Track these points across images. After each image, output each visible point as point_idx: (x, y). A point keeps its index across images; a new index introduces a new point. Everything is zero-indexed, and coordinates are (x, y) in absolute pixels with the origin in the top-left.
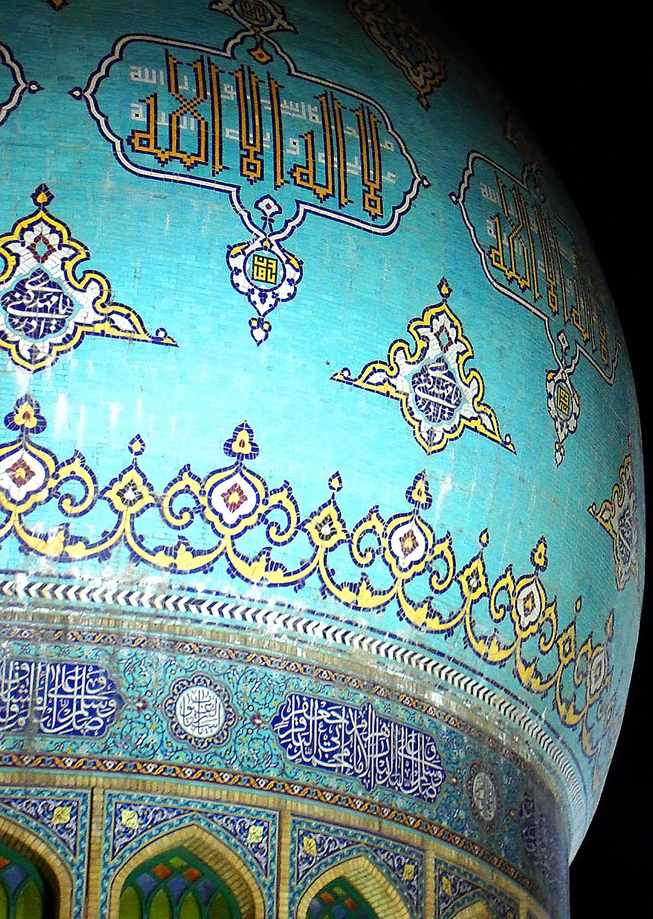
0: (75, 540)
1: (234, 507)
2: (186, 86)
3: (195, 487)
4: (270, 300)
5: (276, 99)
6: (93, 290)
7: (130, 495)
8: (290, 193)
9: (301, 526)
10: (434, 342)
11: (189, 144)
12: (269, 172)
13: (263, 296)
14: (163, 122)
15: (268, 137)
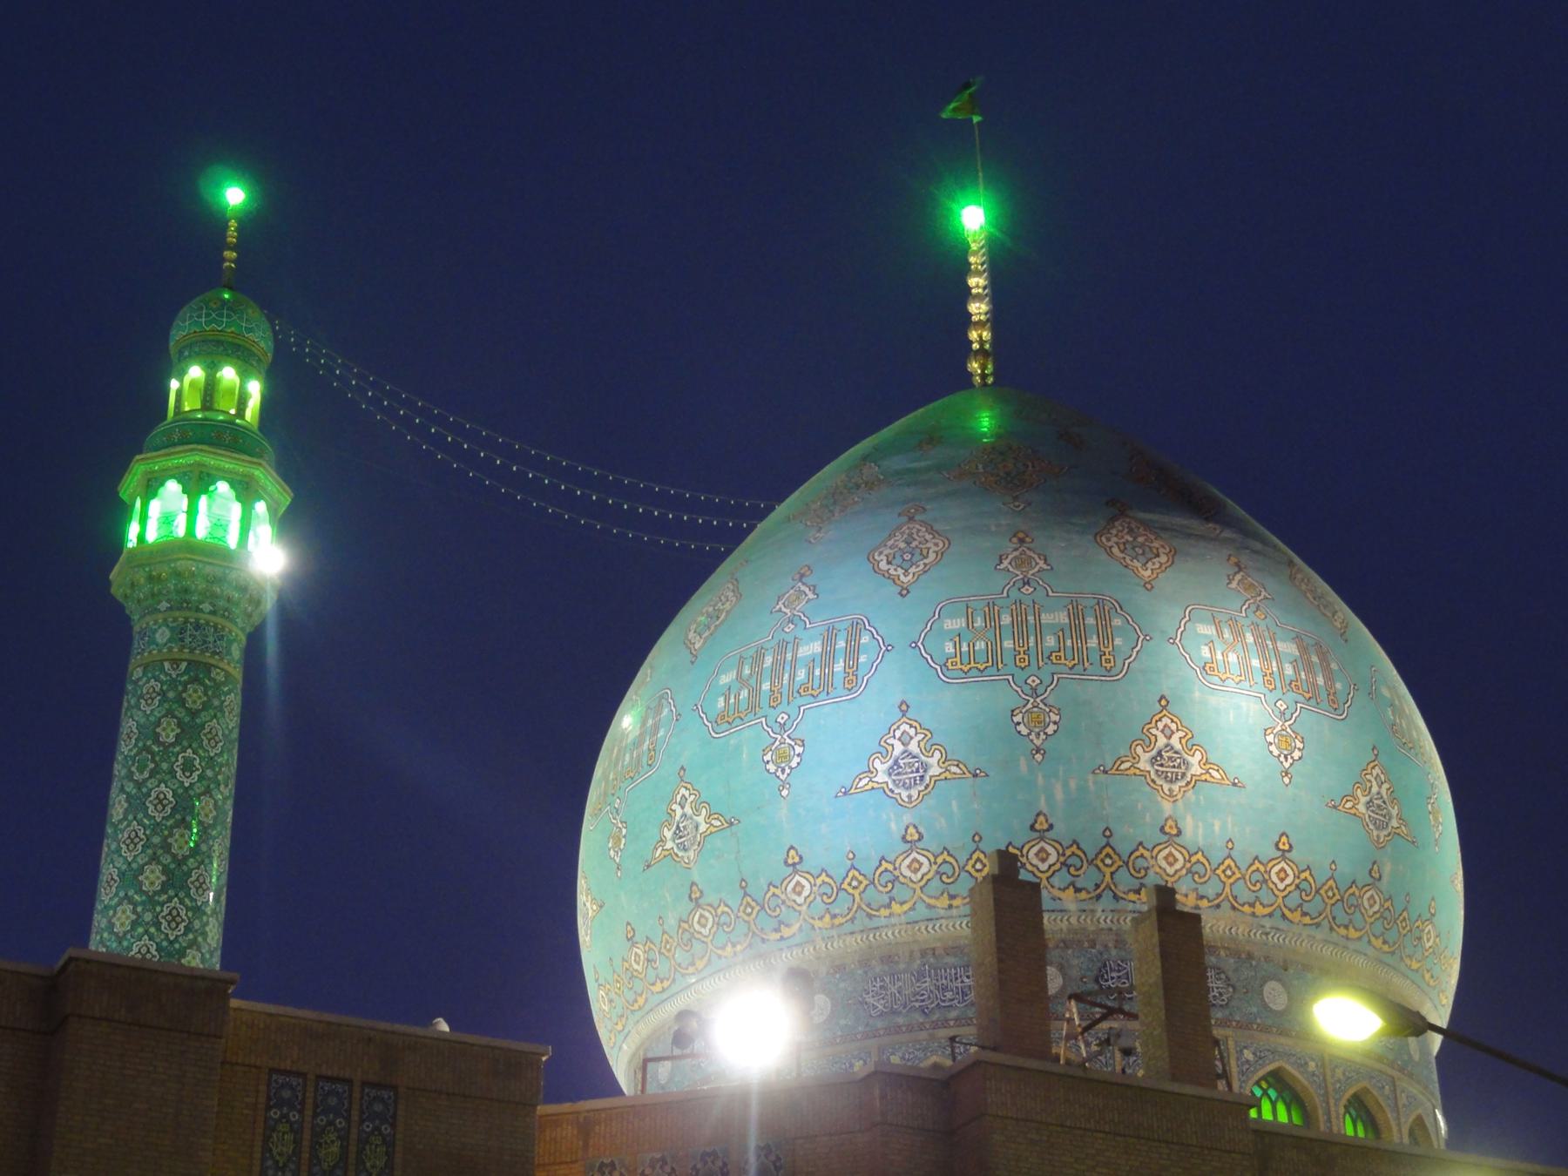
2: (1227, 635)
4: (1043, 736)
6: (937, 755)
7: (1229, 873)
15: (1032, 639)
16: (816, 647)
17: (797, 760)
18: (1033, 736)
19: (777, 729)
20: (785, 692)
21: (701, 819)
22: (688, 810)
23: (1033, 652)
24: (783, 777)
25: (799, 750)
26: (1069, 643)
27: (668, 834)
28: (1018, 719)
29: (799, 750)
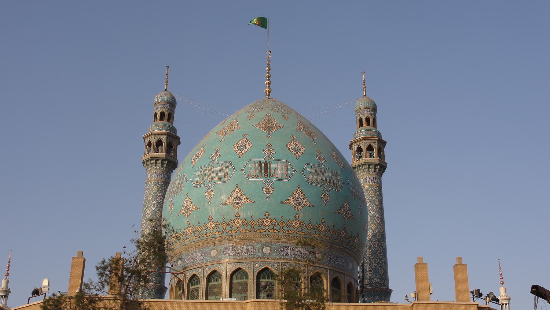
5: (270, 165)
11: (257, 174)
16: (218, 169)
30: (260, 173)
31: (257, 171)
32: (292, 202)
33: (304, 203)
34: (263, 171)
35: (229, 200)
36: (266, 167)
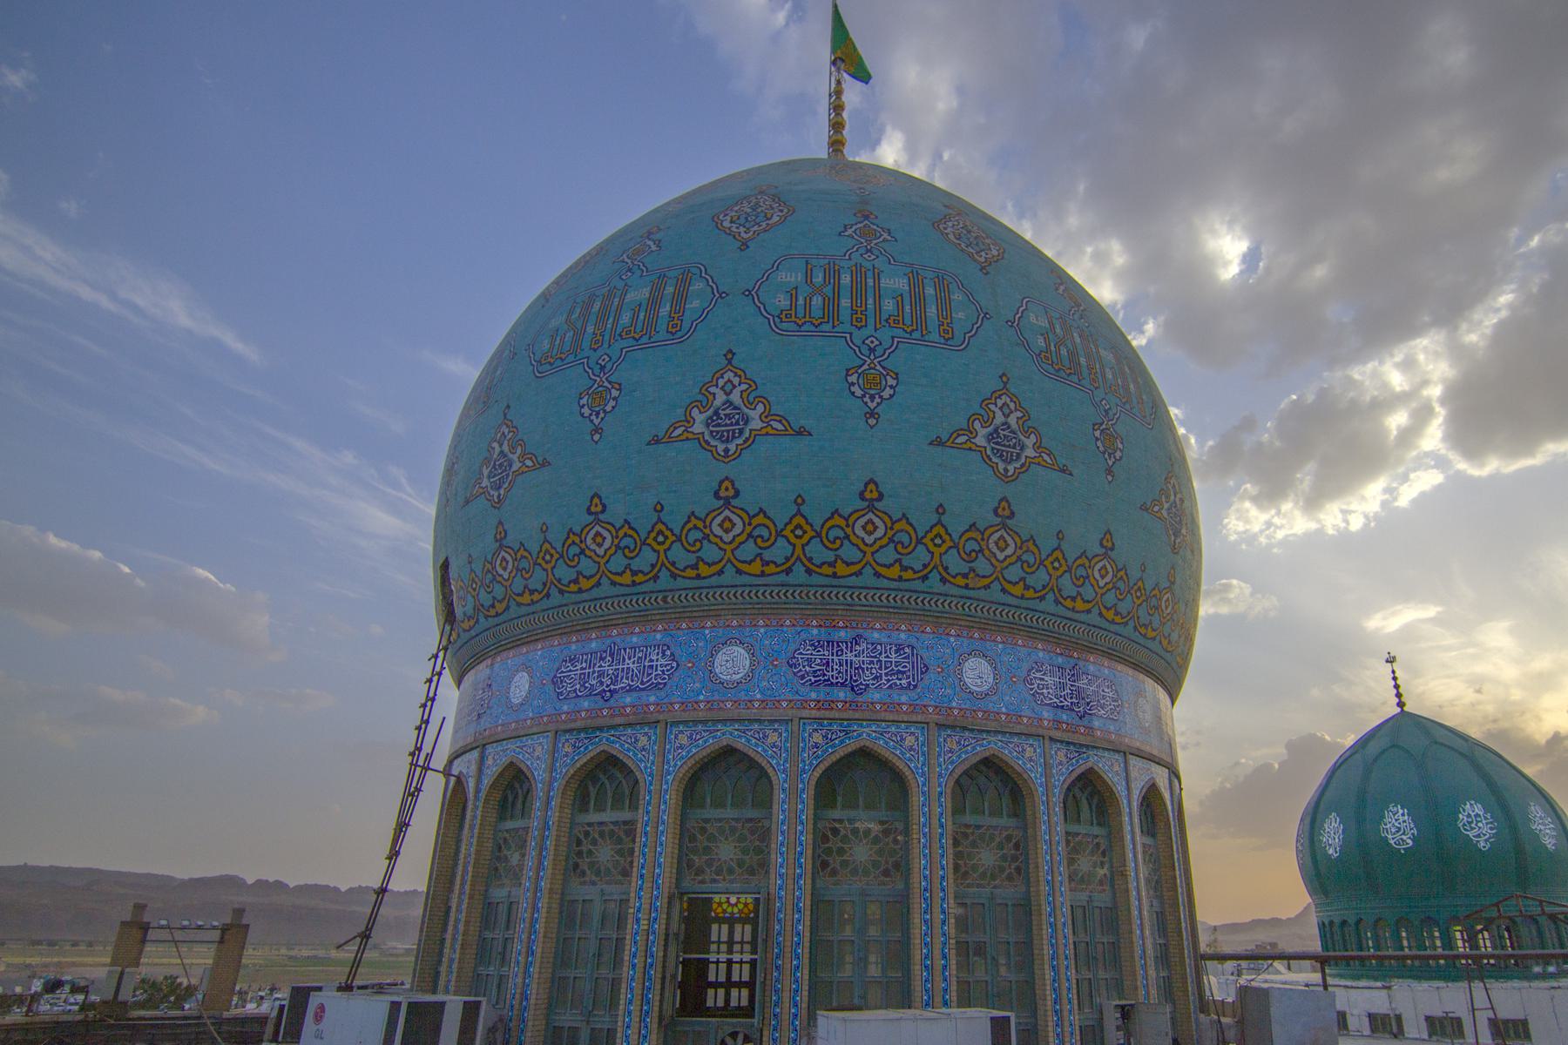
0: (767, 563)
1: (870, 533)
3: (700, 524)
4: (877, 400)
5: (877, 277)
8: (885, 334)
9: (919, 542)
10: (999, 414)
11: (817, 313)
12: (871, 321)
13: (872, 398)
14: (801, 301)
15: (870, 301)
16: (645, 293)
17: (612, 403)
18: (867, 399)
19: (597, 370)
20: (607, 338)
21: (515, 457)
22: (506, 448)
23: (870, 313)
24: (596, 421)
25: (615, 393)
26: (907, 308)
27: (486, 472)
28: (853, 379)
29: (615, 393)
30: (831, 304)
31: (817, 301)
32: (980, 440)
33: (1030, 452)
34: (845, 303)
35: (689, 420)
36: (858, 291)
